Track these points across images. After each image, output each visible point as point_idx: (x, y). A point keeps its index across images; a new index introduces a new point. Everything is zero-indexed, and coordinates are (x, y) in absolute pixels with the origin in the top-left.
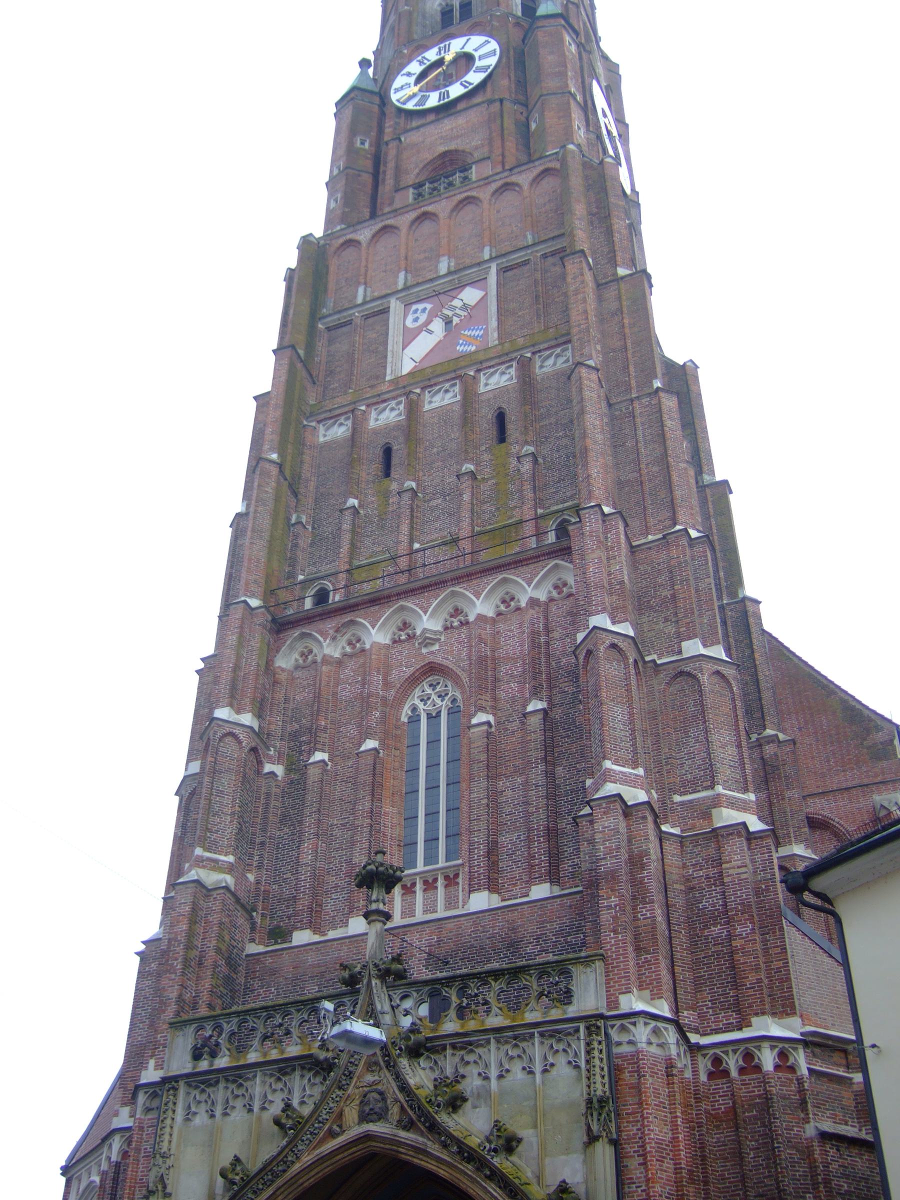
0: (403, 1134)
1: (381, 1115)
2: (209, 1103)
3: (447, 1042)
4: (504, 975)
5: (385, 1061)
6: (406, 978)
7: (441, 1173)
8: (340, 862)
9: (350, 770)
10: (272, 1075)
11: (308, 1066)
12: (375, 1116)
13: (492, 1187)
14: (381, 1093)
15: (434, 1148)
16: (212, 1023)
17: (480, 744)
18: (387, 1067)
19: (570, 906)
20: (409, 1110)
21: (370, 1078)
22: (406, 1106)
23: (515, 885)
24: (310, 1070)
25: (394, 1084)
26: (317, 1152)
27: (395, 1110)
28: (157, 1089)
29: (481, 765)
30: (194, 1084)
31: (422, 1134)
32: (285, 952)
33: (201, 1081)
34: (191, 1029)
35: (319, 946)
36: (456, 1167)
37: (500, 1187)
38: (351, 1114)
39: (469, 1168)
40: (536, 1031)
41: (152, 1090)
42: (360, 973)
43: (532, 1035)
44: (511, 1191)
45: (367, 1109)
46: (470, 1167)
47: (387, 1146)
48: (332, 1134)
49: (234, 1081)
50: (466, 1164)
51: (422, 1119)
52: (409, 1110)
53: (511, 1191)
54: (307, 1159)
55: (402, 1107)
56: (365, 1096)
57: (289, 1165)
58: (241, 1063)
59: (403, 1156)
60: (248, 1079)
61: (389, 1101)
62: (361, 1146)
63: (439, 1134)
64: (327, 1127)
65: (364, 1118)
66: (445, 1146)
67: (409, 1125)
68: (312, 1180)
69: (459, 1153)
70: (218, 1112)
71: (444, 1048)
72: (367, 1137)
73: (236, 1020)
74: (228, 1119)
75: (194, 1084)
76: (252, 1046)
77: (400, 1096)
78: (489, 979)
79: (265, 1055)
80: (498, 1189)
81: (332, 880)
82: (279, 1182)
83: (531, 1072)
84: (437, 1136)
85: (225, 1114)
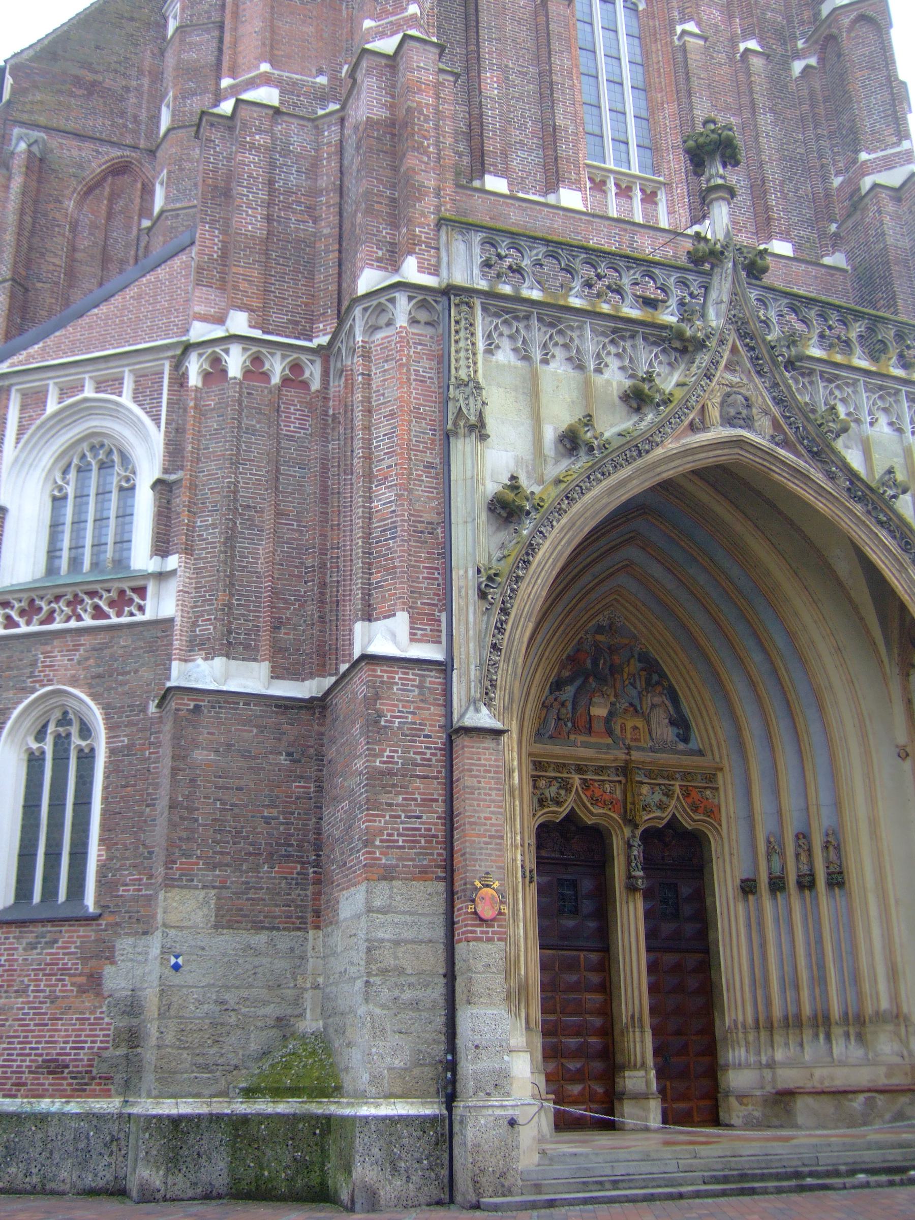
0: (782, 452)
1: (748, 423)
2: (521, 340)
3: (818, 367)
4: (863, 318)
5: (755, 366)
6: (760, 280)
7: (821, 506)
8: (523, 116)
9: (522, 10)
10: (603, 334)
11: (652, 339)
12: (742, 422)
13: (883, 534)
14: (747, 399)
15: (818, 476)
16: (508, 241)
17: (698, 58)
18: (758, 373)
19: (816, 277)
20: (786, 428)
21: (729, 376)
22: (782, 421)
23: (740, 231)
24: (654, 343)
25: (765, 393)
26: (683, 441)
27: (765, 423)
28: (429, 299)
29: (702, 82)
30: (493, 309)
31: (798, 455)
32: (477, 195)
33: (508, 310)
34: (477, 238)
35: (524, 205)
36: (843, 503)
37: (894, 537)
38: (714, 413)
39: (858, 509)
40: (904, 389)
41: (420, 297)
42: (722, 253)
43: (898, 392)
44: (907, 543)
45: (732, 412)
46: (859, 507)
47: (757, 460)
48: (692, 427)
49: (551, 325)
50: (855, 504)
51: (805, 442)
52: (786, 428)
53: (907, 543)
54: (671, 446)
55: (776, 425)
56: (728, 395)
57: (653, 444)
58: (562, 302)
59: (777, 476)
60: (572, 328)
61: (754, 411)
62: (726, 451)
63: (823, 462)
64: (691, 417)
65: (729, 421)
66: (832, 477)
67: (786, 444)
68: (671, 472)
69: (849, 490)
70: (538, 355)
71: (811, 372)
72: (739, 442)
73: (544, 249)
74: (545, 367)
75: (493, 309)
76: (571, 289)
77: (775, 410)
78: (849, 317)
79: (594, 305)
80: (890, 538)
81: (516, 135)
82: (639, 462)
83: (900, 431)
84: (819, 465)
85: (545, 362)
